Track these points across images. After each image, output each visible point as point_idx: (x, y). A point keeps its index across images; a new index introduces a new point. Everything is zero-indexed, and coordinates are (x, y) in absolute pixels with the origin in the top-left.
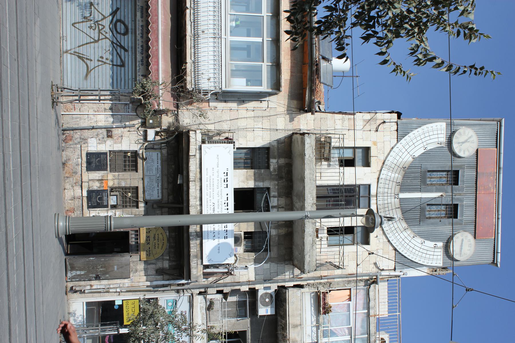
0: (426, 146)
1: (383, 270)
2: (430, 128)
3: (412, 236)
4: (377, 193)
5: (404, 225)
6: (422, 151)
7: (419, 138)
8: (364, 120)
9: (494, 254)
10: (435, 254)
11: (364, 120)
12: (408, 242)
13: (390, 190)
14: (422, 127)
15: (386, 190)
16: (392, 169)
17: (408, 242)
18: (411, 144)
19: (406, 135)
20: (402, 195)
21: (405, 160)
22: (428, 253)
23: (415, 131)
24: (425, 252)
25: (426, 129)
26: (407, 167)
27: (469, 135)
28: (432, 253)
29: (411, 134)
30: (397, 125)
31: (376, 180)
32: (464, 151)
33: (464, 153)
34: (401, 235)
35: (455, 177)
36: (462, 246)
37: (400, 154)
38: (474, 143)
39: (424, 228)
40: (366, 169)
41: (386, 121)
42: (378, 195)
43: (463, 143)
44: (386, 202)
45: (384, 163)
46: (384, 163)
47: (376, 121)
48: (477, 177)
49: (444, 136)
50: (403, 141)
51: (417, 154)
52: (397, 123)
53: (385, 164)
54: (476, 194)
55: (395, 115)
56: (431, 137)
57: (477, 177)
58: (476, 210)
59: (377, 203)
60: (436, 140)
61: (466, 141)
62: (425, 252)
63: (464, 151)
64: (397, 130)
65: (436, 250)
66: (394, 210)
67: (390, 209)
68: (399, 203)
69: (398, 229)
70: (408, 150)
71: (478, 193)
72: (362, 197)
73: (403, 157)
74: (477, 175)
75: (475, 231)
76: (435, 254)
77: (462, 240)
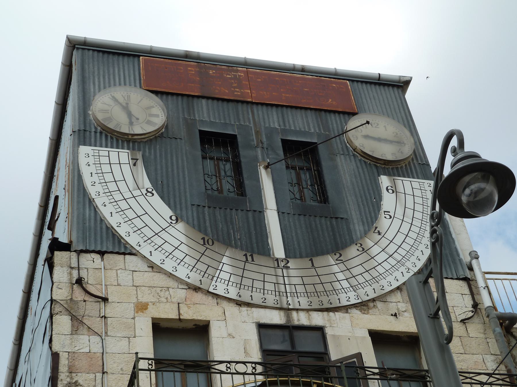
0: (144, 192)
1: (475, 306)
2: (95, 178)
3: (377, 237)
4: (281, 309)
5: (353, 251)
6: (156, 200)
7: (123, 205)
8: (75, 331)
9: (384, 85)
10: (409, 191)
11: (75, 331)
12: (392, 248)
13: (268, 278)
14: (93, 196)
15: (269, 287)
16: (210, 271)
17: (392, 248)
18: (138, 223)
19: (114, 235)
20: (279, 252)
21: (183, 239)
22: (410, 204)
23: (105, 212)
24: (409, 212)
25: (98, 188)
26: (204, 236)
27: (112, 103)
28: (410, 199)
29: (113, 221)
30: (87, 251)
31: (244, 309)
32: (151, 115)
33: (157, 116)
34: (380, 258)
35: (218, 143)
36: (379, 140)
37: (168, 248)
38: (129, 97)
39: (352, 209)
40: (216, 332)
41: (75, 275)
42: (285, 306)
43: (130, 115)
44: (300, 289)
45: (197, 289)
46: (197, 289)
47: (77, 302)
48: (213, 99)
49: (114, 153)
50: (133, 240)
51: (167, 212)
52: (82, 251)
53: (198, 284)
54: (252, 103)
55: (59, 256)
56: (118, 176)
57: (213, 99)
58: (292, 107)
59: (308, 310)
60: (126, 169)
61: (126, 108)
62: (409, 212)
63: (151, 115)
64: (102, 253)
65: (400, 188)
66: (320, 271)
67: (317, 280)
68: (298, 260)
69: (367, 266)
70: (157, 229)
71: (250, 100)
72: (293, 345)
73: (176, 243)
74: (208, 98)
75: (339, 113)
76: (409, 191)
77: (367, 137)
